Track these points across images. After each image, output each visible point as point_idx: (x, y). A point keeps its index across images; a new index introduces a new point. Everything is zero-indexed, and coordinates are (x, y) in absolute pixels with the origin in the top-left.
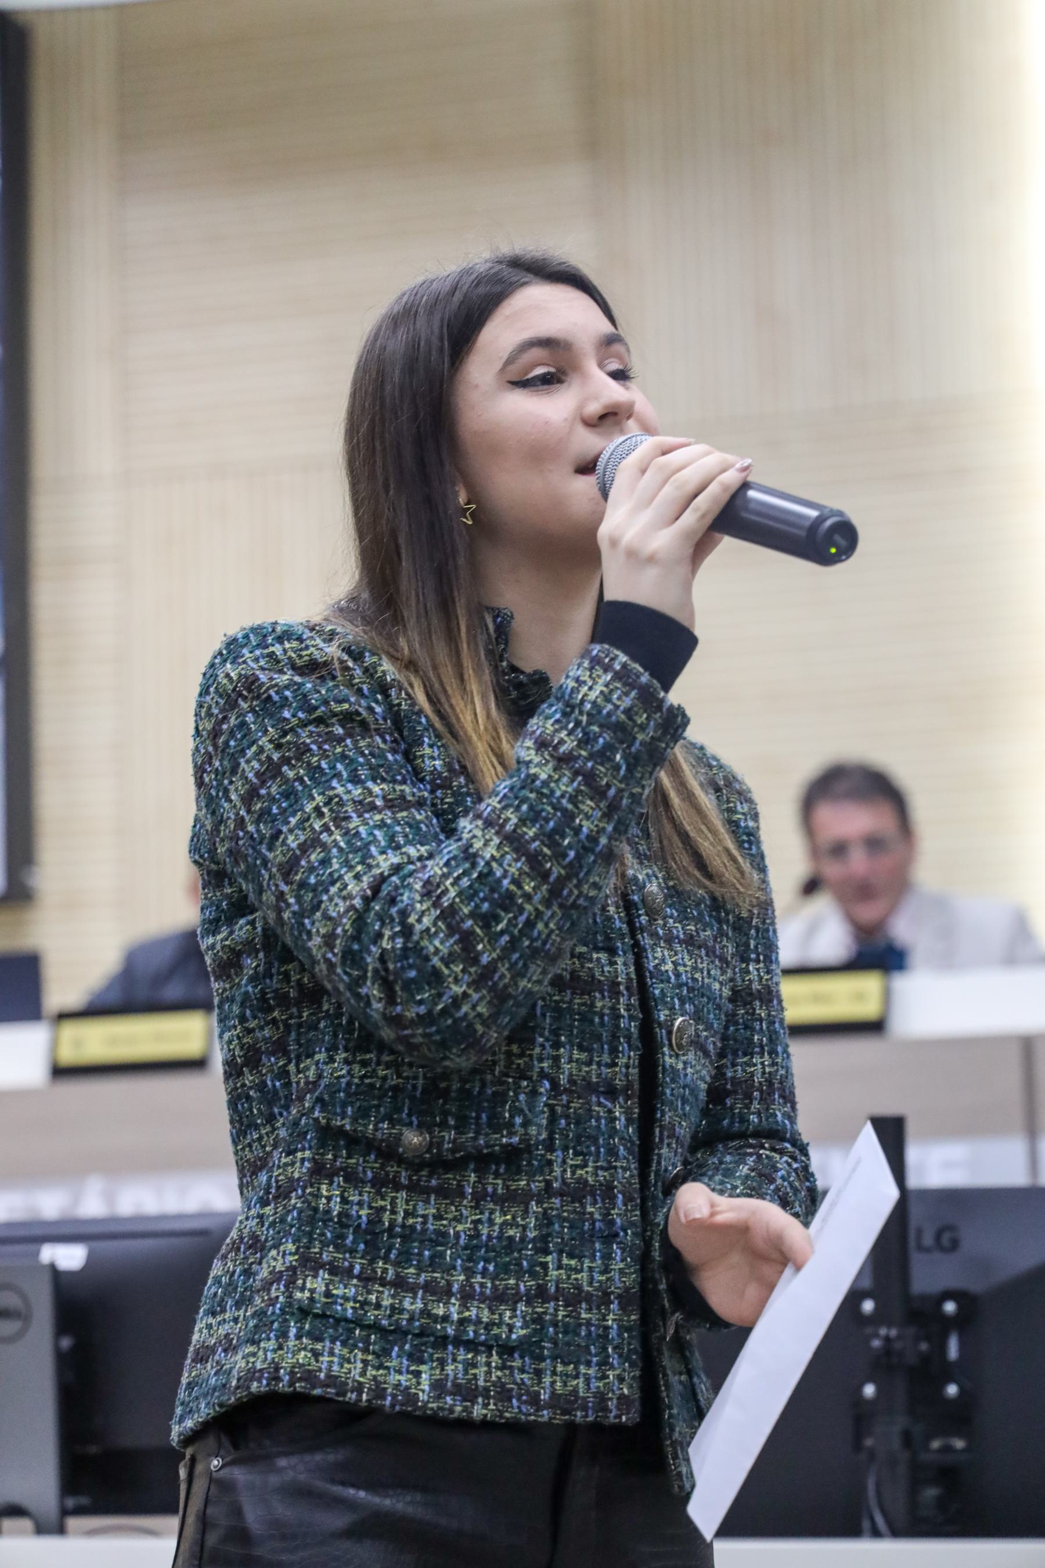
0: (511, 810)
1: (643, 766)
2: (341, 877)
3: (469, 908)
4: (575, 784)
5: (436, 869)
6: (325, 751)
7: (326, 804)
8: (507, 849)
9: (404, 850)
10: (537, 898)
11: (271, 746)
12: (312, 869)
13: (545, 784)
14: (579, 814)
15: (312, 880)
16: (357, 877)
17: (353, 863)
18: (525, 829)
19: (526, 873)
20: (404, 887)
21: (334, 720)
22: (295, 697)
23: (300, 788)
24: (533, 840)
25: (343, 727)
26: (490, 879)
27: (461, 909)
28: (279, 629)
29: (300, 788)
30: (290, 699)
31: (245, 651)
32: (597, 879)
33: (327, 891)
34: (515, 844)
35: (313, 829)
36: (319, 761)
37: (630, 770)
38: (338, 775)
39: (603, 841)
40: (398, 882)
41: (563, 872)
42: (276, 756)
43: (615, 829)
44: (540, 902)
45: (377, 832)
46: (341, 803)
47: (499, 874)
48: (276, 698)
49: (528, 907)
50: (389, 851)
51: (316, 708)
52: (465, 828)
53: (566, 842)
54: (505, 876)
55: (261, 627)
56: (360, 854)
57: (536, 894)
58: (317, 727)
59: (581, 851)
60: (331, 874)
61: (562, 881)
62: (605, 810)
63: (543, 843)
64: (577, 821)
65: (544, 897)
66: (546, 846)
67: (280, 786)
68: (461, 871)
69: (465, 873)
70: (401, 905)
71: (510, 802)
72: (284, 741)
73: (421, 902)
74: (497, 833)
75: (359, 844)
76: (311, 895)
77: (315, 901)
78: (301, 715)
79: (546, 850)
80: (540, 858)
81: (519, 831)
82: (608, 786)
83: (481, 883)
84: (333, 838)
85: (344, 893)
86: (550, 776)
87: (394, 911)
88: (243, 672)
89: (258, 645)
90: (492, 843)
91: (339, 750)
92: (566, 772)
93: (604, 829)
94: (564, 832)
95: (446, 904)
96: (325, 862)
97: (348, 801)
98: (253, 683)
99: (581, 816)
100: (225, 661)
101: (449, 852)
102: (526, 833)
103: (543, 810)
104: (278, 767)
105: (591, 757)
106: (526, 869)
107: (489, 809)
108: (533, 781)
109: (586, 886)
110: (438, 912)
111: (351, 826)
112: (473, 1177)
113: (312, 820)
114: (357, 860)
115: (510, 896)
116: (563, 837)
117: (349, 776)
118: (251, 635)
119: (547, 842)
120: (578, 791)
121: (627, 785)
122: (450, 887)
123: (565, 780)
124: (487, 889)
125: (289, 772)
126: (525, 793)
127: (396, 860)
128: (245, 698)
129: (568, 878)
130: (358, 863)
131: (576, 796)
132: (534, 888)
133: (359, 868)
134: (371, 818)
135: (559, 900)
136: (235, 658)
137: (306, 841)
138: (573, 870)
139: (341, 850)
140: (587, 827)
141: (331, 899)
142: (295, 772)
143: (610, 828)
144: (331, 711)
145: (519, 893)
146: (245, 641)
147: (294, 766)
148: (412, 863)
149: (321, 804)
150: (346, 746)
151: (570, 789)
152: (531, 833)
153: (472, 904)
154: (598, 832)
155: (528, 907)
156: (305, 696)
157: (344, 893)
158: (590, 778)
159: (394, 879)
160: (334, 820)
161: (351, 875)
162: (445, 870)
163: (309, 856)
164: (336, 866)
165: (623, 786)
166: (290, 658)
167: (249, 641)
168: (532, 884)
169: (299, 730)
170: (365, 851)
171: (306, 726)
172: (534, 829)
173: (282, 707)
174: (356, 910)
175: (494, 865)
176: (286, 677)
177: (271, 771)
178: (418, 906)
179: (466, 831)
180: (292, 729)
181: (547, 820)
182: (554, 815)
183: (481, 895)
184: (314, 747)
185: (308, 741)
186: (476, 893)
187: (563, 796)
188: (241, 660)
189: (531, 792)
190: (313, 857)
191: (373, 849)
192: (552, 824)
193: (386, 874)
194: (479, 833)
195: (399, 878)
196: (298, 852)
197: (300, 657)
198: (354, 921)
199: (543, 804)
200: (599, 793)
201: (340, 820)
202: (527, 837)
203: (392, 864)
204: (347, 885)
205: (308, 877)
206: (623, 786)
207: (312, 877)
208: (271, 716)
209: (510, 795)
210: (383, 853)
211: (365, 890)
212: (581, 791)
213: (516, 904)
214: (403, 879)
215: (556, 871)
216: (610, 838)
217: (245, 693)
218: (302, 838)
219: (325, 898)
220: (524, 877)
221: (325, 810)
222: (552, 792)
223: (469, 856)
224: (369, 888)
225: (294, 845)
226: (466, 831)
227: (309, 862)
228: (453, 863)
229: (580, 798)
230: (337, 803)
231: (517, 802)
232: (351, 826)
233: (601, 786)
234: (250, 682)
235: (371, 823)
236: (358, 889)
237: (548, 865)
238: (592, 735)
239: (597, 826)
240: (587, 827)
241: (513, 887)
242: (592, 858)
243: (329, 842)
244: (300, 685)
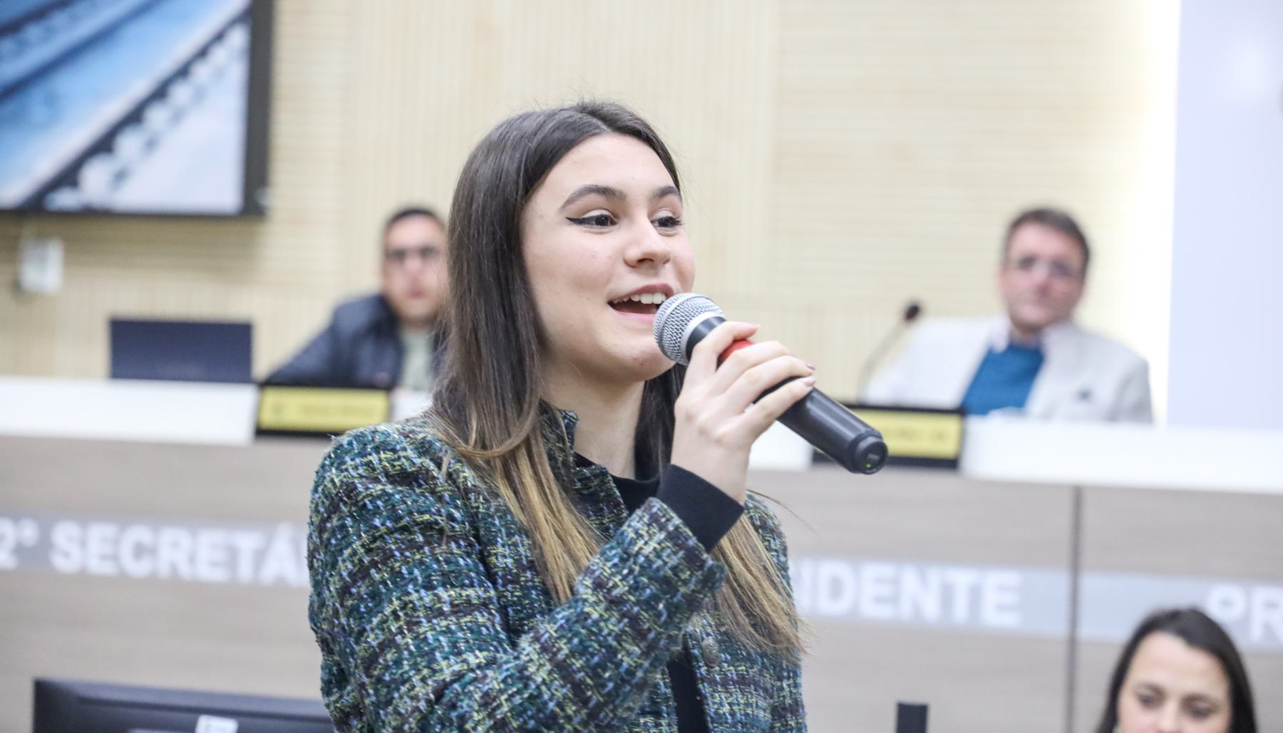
0: (565, 641)
1: (681, 614)
2: (409, 679)
3: (518, 723)
4: (621, 625)
5: (495, 682)
6: (407, 557)
7: (403, 608)
8: (556, 676)
9: (464, 656)
10: (576, 720)
11: (362, 550)
12: (387, 668)
13: (596, 623)
14: (621, 650)
15: (387, 678)
16: (423, 680)
17: (420, 667)
18: (573, 660)
19: (570, 699)
20: (465, 694)
21: (416, 529)
23: (384, 591)
24: (579, 670)
25: (423, 535)
26: (539, 701)
27: (511, 723)
28: (378, 438)
29: (384, 591)
30: (382, 508)
31: (347, 459)
32: (631, 704)
33: (398, 689)
34: (564, 673)
35: (390, 630)
36: (400, 567)
37: (670, 616)
38: (414, 580)
39: (640, 674)
40: (459, 689)
41: (601, 699)
42: (366, 560)
43: (651, 665)
44: (579, 723)
45: (441, 638)
46: (414, 609)
47: (546, 697)
48: (370, 506)
49: (568, 727)
50: (451, 657)
51: (401, 518)
52: (524, 649)
53: (607, 675)
54: (551, 700)
55: (363, 435)
56: (426, 658)
57: (576, 716)
58: (400, 534)
59: (619, 682)
60: (402, 675)
61: (600, 706)
62: (645, 650)
63: (587, 674)
64: (619, 656)
65: (583, 719)
66: (589, 677)
67: (367, 587)
68: (515, 689)
69: (519, 692)
70: (460, 711)
71: (564, 633)
73: (477, 712)
74: (550, 660)
75: (426, 648)
76: (385, 690)
77: (389, 697)
78: (389, 524)
79: (589, 681)
80: (583, 687)
81: (568, 661)
82: (649, 630)
83: (532, 704)
84: (405, 640)
85: (412, 693)
86: (601, 616)
87: (454, 714)
88: (345, 480)
89: (359, 453)
90: (545, 668)
91: (418, 557)
92: (615, 614)
93: (641, 665)
94: (607, 666)
95: (499, 717)
96: (398, 663)
97: (420, 607)
98: (352, 491)
99: (623, 653)
100: (332, 464)
101: (507, 670)
102: (574, 664)
103: (591, 646)
104: (368, 569)
105: (637, 603)
106: (570, 695)
107: (547, 635)
108: (586, 619)
109: (620, 710)
110: (492, 722)
111: (421, 630)
113: (390, 622)
114: (424, 664)
115: (554, 716)
116: (605, 670)
117: (423, 582)
118: (355, 443)
119: (590, 674)
120: (623, 632)
121: (666, 629)
122: (504, 702)
123: (613, 620)
124: (534, 709)
125: (376, 575)
126: (578, 627)
127: (457, 668)
128: (345, 503)
129: (605, 704)
130: (424, 667)
131: (620, 636)
132: (575, 712)
133: (425, 672)
134: (438, 624)
135: (596, 722)
136: (340, 464)
137: (384, 640)
138: (611, 697)
139: (411, 653)
140: (627, 662)
141: (401, 697)
142: (381, 575)
143: (646, 664)
144: (414, 521)
145: (562, 714)
146: (350, 447)
147: (380, 569)
148: (472, 670)
149: (398, 608)
150: (424, 553)
151: (616, 629)
152: (578, 664)
153: (521, 720)
154: (636, 667)
155: (568, 727)
156: (394, 506)
157: (412, 693)
158: (634, 620)
159: (456, 686)
160: (408, 623)
161: (418, 677)
162: (502, 686)
163: (386, 654)
164: (406, 668)
165: (662, 630)
166: (384, 467)
167: (353, 449)
168: (574, 708)
169: (386, 536)
170: (431, 656)
171: (392, 533)
172: (581, 662)
173: (374, 514)
174: (420, 711)
175: (544, 688)
176: (380, 487)
177: (361, 573)
178: (475, 714)
179: (525, 653)
180: (381, 536)
181: (593, 655)
182: (600, 651)
183: (529, 713)
184: (397, 553)
185: (393, 547)
186: (525, 711)
187: (609, 634)
188: (344, 467)
189: (583, 628)
190: (389, 656)
191: (438, 654)
192: (596, 659)
193: (448, 680)
194: (535, 657)
195: (460, 686)
196: (377, 650)
197: (394, 466)
198: (419, 721)
199: (592, 640)
200: (640, 635)
201: (412, 624)
202: (574, 667)
203: (454, 671)
204: (415, 686)
205: (384, 675)
206: (662, 630)
207: (387, 674)
208: (366, 521)
209: (565, 626)
210: (446, 658)
211: (427, 694)
212: (626, 632)
213: (558, 724)
214: (464, 687)
215: (595, 698)
216: (646, 671)
217: (345, 499)
218: (382, 637)
219: (396, 695)
220: (567, 701)
221: (401, 614)
222: (601, 630)
223: (522, 676)
224: (433, 693)
225: (374, 643)
226: (525, 653)
227: (385, 660)
228: (509, 681)
229: (624, 637)
230: (412, 608)
231: (570, 635)
232: (421, 630)
233: (643, 630)
234: (350, 489)
235: (438, 629)
236: (424, 691)
237: (589, 693)
238: (641, 585)
239: (636, 662)
240: (627, 662)
241: (557, 710)
242: (628, 688)
243: (402, 644)
244: (390, 495)
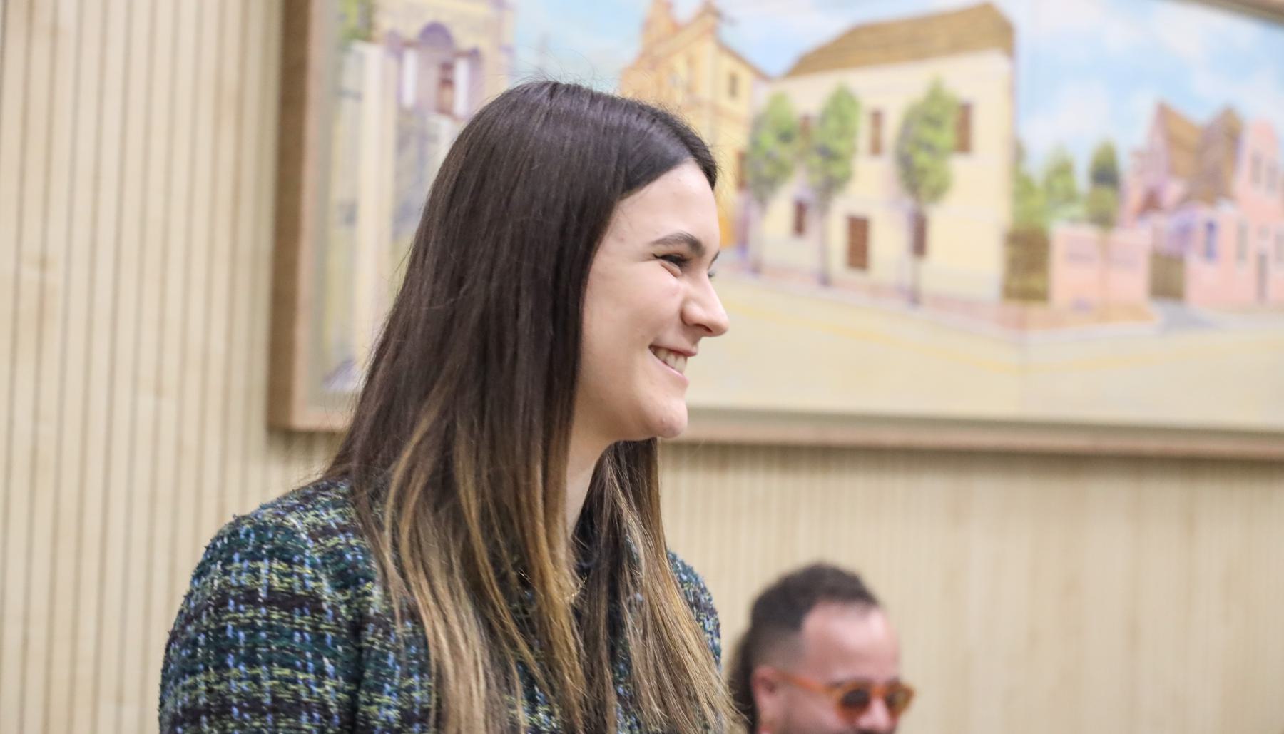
22: (246, 643)
36: (233, 729)
42: (202, 701)
48: (230, 634)
72: (216, 687)
118: (253, 536)
128: (208, 615)
217: (211, 610)
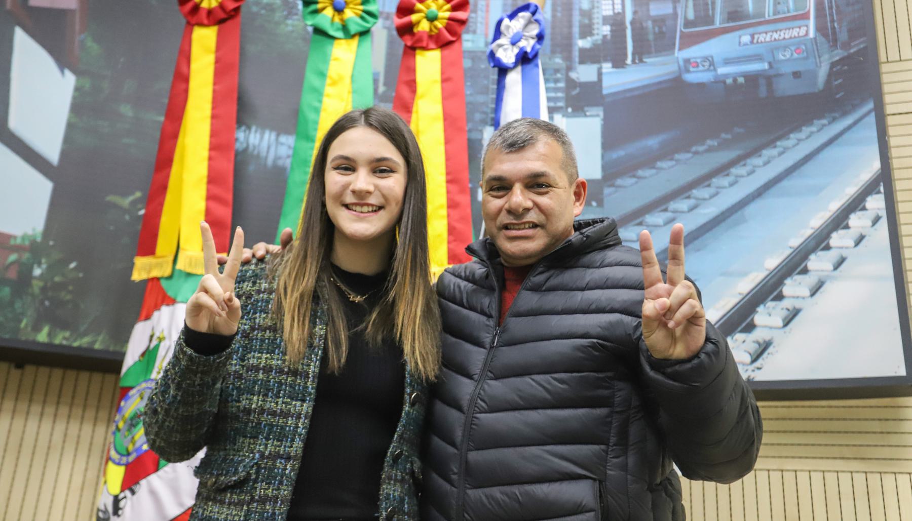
112: (229, 495)
